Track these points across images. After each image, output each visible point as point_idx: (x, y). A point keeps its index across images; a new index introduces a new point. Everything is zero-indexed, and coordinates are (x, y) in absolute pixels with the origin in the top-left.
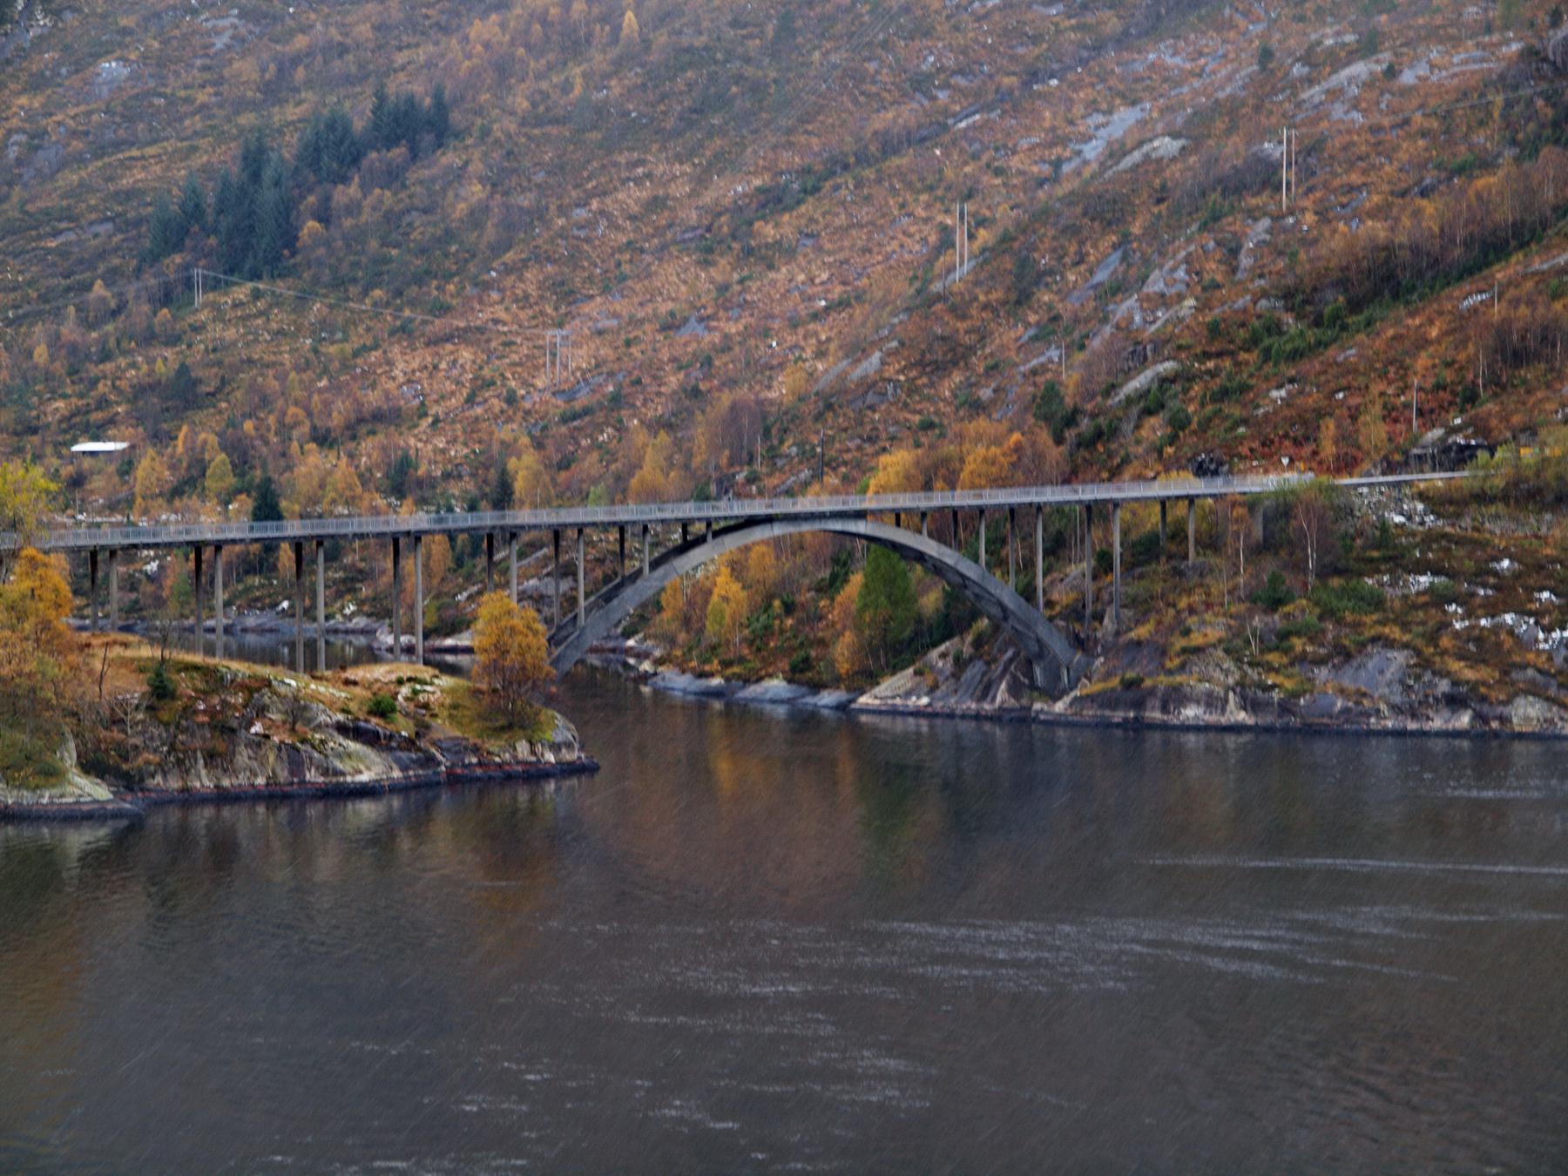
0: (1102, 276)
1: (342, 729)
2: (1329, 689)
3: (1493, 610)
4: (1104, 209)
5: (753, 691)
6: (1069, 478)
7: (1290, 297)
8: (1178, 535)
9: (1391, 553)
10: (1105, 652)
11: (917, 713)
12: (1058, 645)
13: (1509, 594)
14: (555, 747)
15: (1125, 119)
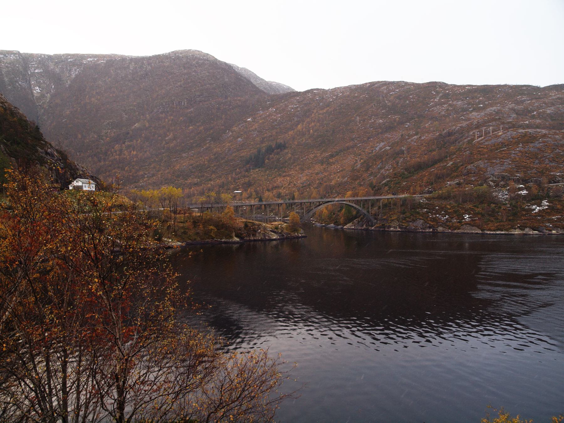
1: (271, 231)
2: (412, 226)
3: (435, 214)
4: (379, 157)
5: (329, 226)
6: (374, 195)
7: (406, 169)
8: (390, 203)
9: (421, 206)
11: (352, 229)
12: (373, 219)
13: (438, 212)
15: (382, 144)
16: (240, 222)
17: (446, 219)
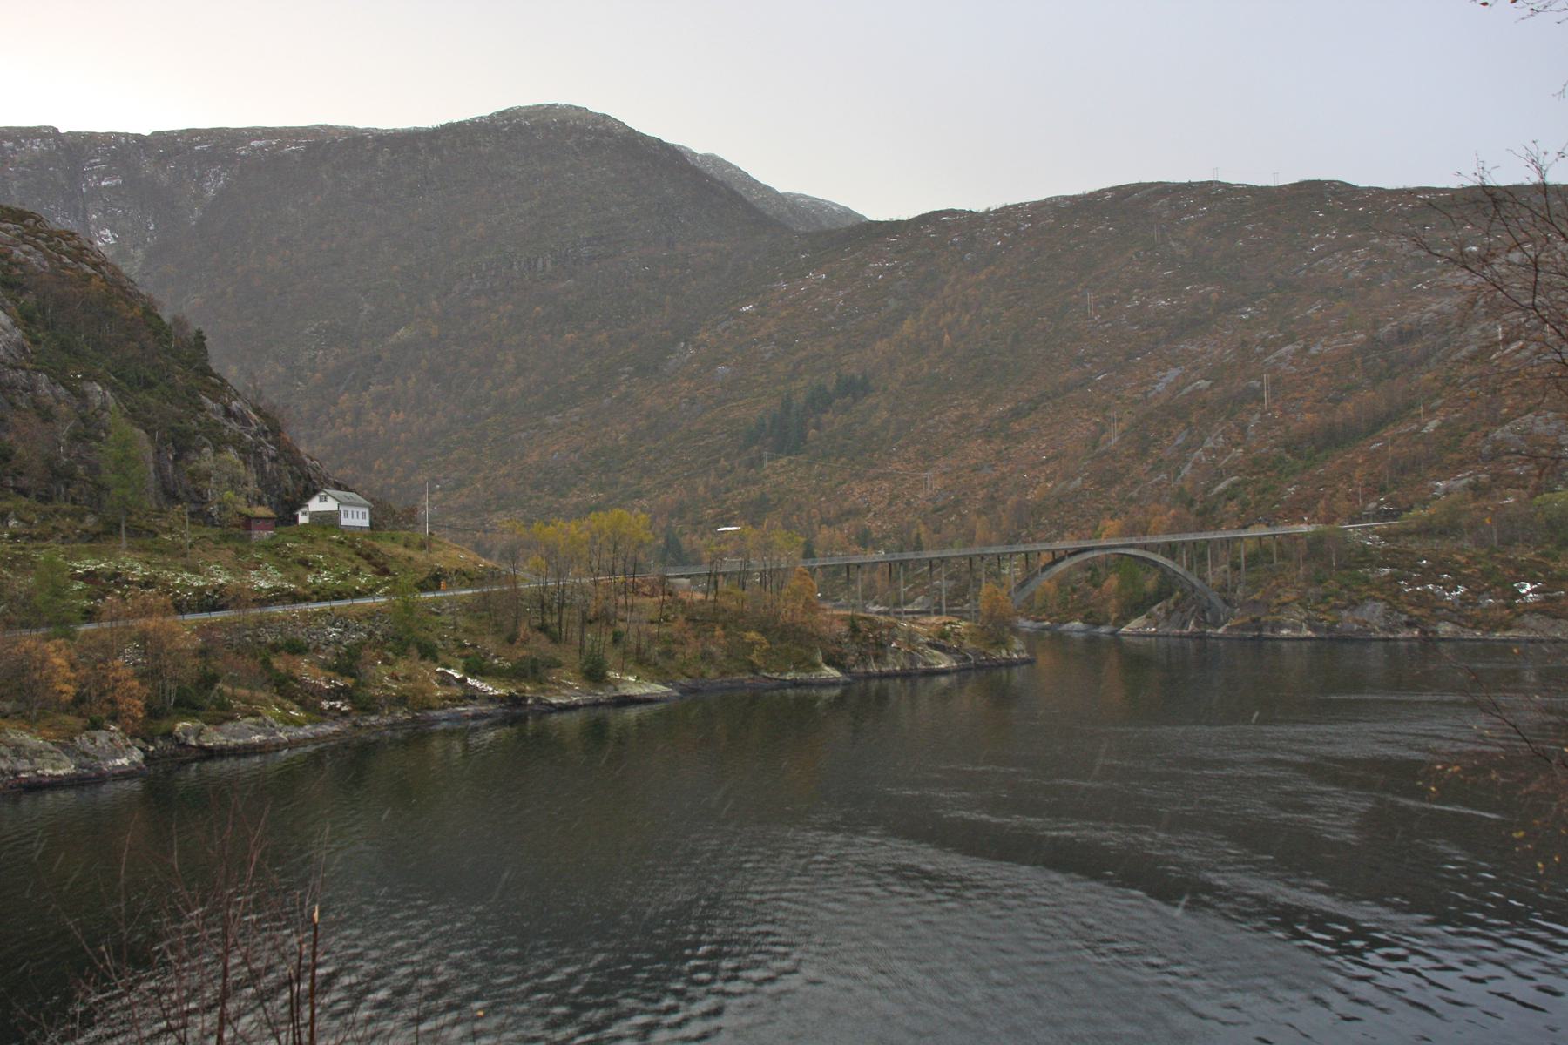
0: (1179, 441)
1: (929, 644)
2: (1349, 621)
3: (1422, 583)
5: (1065, 627)
8: (1268, 553)
9: (1367, 557)
10: (1241, 605)
11: (1151, 635)
12: (1219, 603)
13: (1430, 575)
14: (1017, 652)
15: (1173, 373)
16: (833, 617)
17: (1461, 597)
